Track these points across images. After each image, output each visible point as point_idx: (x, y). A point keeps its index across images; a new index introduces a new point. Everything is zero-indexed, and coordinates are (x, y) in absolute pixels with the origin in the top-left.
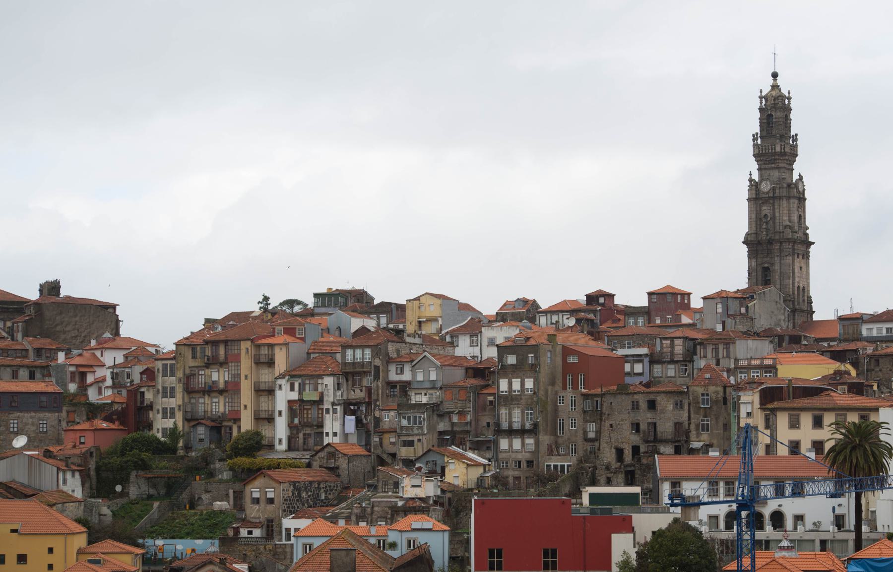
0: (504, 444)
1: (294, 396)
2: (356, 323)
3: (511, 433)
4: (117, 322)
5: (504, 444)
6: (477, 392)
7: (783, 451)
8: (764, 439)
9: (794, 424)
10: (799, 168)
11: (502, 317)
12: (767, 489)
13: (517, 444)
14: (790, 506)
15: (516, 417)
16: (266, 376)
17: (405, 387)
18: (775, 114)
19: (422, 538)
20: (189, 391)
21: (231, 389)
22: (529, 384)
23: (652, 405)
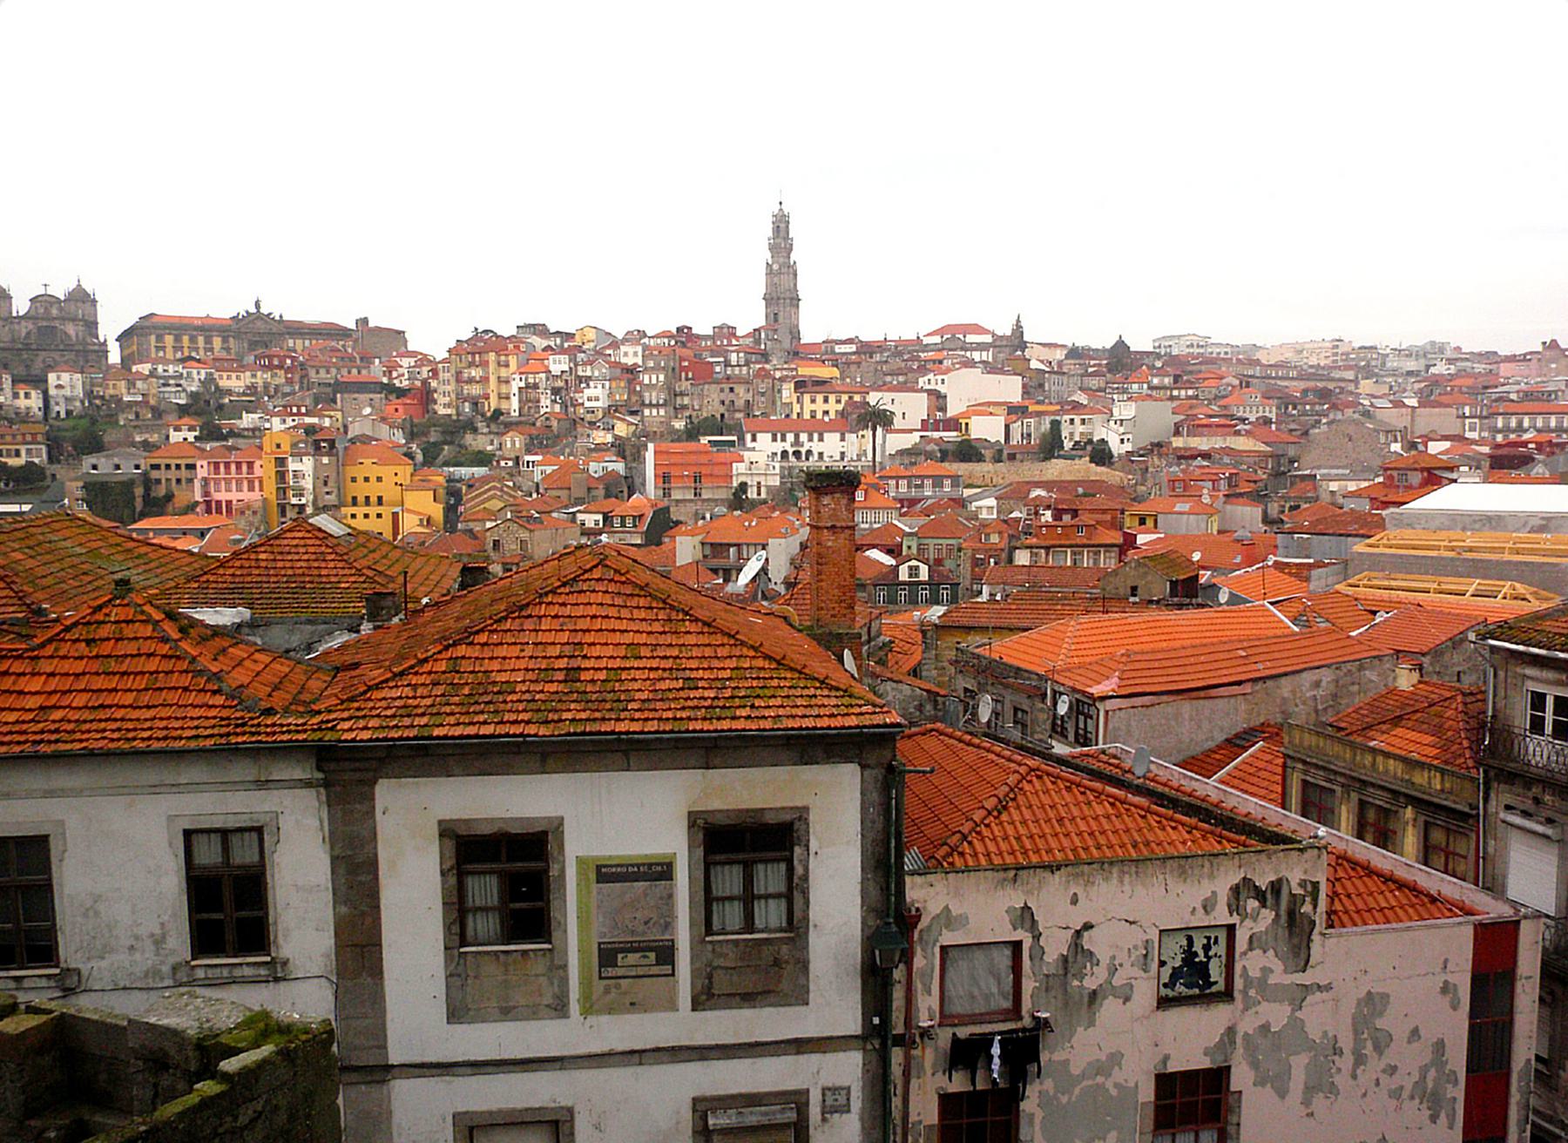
0: (647, 412)
1: (522, 384)
2: (545, 343)
3: (651, 405)
4: (406, 341)
5: (647, 412)
6: (630, 382)
7: (807, 416)
8: (797, 408)
9: (813, 401)
10: (793, 257)
11: (625, 340)
12: (804, 437)
13: (654, 412)
14: (816, 447)
15: (651, 397)
16: (504, 373)
17: (589, 379)
18: (781, 226)
19: (611, 466)
20: (458, 381)
21: (485, 380)
22: (662, 377)
23: (732, 390)
